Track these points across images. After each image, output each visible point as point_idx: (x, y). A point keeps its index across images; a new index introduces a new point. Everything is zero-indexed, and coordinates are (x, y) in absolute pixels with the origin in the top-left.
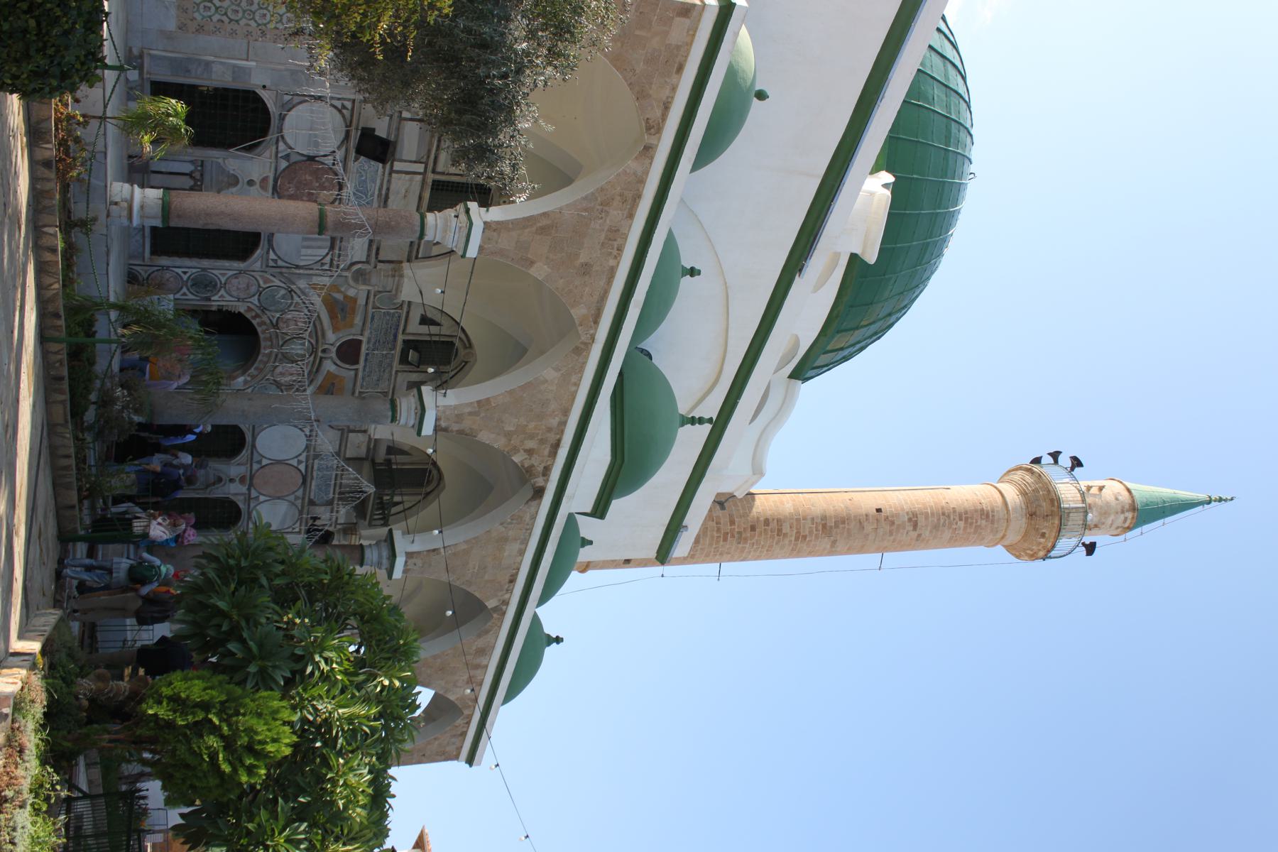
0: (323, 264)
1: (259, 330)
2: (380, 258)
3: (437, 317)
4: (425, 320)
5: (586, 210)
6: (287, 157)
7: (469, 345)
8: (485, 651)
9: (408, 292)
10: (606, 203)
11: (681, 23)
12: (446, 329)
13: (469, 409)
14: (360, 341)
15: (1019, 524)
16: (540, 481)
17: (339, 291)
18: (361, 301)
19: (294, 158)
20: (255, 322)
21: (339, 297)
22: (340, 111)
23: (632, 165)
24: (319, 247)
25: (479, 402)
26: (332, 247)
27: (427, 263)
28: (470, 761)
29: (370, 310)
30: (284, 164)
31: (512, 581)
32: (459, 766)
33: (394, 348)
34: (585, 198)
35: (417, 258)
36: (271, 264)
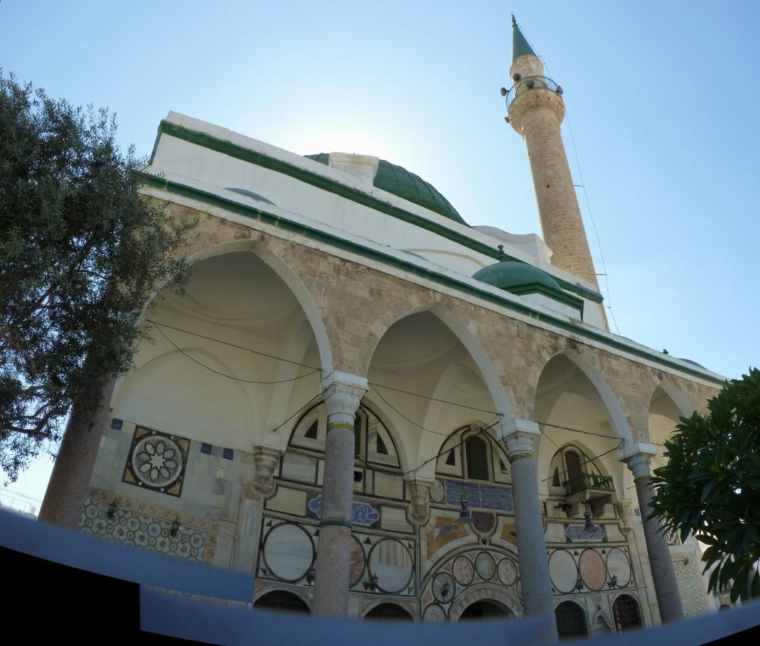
0: (410, 546)
1: (472, 601)
2: (401, 498)
4: (451, 461)
5: (320, 289)
7: (467, 428)
9: (427, 474)
10: (314, 273)
12: (456, 440)
13: (512, 394)
14: (473, 512)
17: (433, 531)
18: (440, 513)
20: (466, 606)
21: (437, 531)
22: (274, 527)
24: (395, 548)
25: (504, 385)
26: (396, 539)
27: (403, 461)
29: (447, 505)
33: (476, 485)
34: (309, 290)
35: (399, 468)
36: (412, 593)
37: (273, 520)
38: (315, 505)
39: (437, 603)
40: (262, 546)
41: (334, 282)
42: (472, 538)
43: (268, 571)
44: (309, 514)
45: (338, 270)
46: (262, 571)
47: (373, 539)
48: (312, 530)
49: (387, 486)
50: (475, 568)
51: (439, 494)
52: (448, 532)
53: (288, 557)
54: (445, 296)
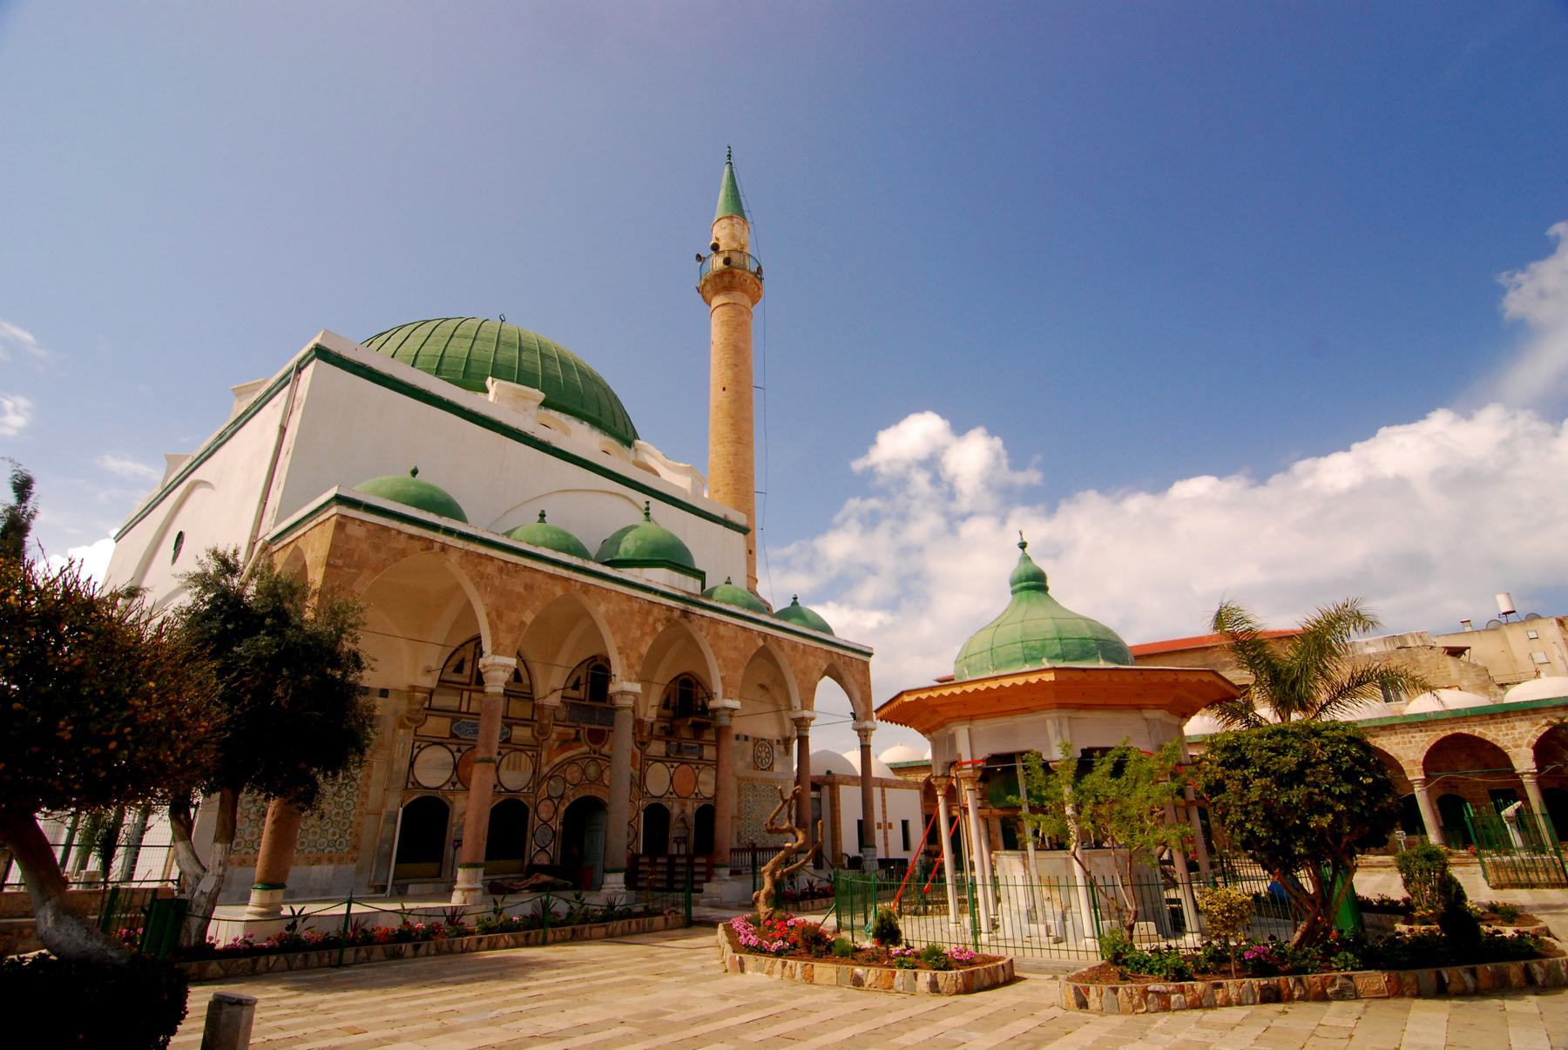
3: (574, 677)
4: (576, 687)
6: (454, 784)
8: (794, 646)
9: (554, 700)
10: (482, 576)
11: (352, 529)
15: (737, 296)
16: (676, 614)
18: (561, 729)
19: (455, 779)
23: (454, 558)
28: (870, 655)
30: (459, 786)
31: (744, 629)
32: (873, 661)
37: (425, 741)
38: (458, 728)
39: (550, 798)
40: (412, 764)
41: (497, 582)
42: (585, 749)
43: (417, 784)
44: (453, 736)
45: (501, 570)
46: (411, 783)
47: (504, 752)
48: (454, 748)
49: (520, 709)
50: (584, 771)
51: (562, 715)
52: (565, 744)
53: (433, 771)
54: (584, 585)
